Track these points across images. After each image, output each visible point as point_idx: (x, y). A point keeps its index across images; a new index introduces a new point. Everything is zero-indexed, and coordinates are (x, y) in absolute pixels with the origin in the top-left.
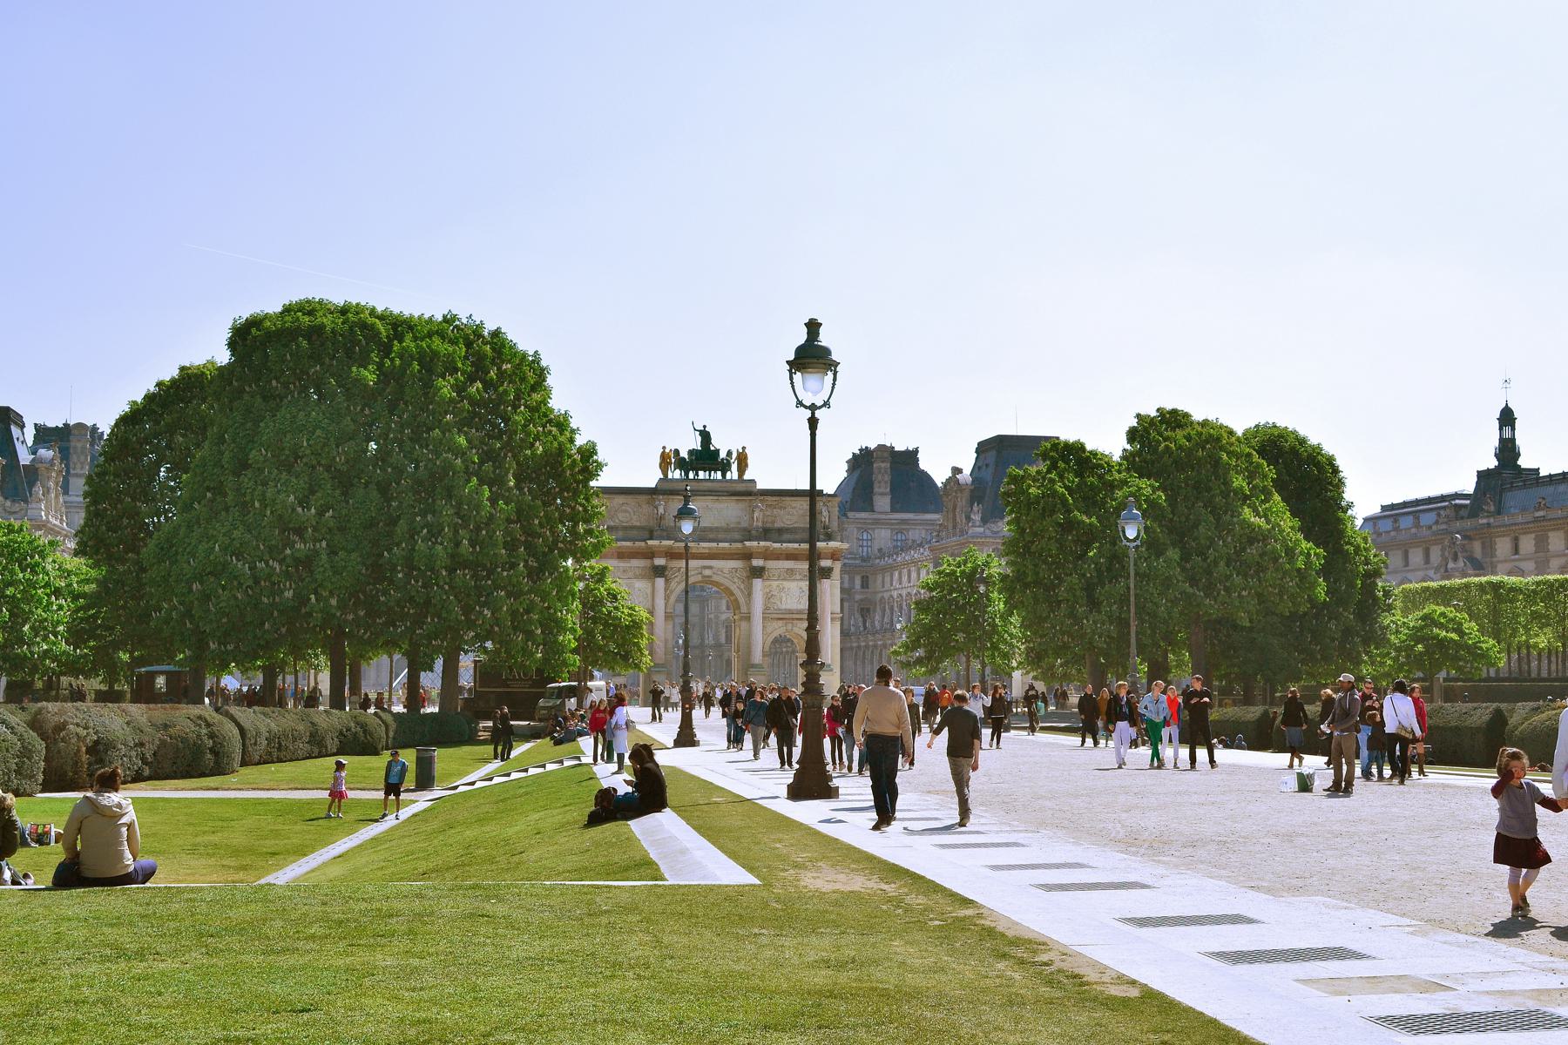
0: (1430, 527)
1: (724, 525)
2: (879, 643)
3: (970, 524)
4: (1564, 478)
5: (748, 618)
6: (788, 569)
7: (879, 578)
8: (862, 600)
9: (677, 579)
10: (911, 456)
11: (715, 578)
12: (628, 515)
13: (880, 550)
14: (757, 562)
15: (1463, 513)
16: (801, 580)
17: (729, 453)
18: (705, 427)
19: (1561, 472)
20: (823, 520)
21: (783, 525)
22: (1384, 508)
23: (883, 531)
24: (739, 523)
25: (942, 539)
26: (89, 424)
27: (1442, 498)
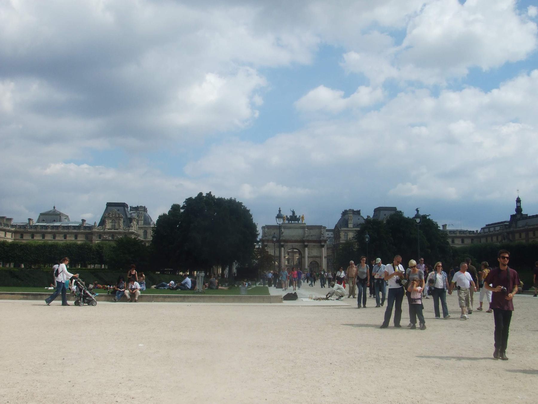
0: (498, 231)
4: (537, 216)
5: (304, 257)
11: (296, 248)
13: (350, 238)
14: (306, 244)
15: (507, 227)
16: (317, 248)
17: (300, 216)
18: (293, 210)
19: (532, 215)
22: (487, 225)
26: (143, 206)
27: (502, 222)
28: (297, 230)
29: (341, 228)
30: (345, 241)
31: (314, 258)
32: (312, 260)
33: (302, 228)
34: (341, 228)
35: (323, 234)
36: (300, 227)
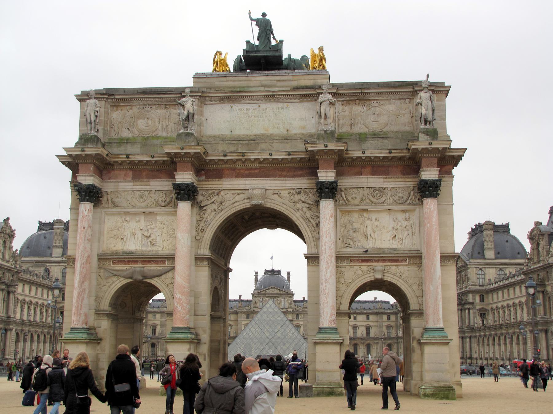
1: (285, 132)
2: (493, 333)
3: (550, 255)
6: (376, 189)
7: (490, 295)
8: (481, 309)
9: (214, 206)
10: (505, 228)
12: (150, 121)
13: (490, 280)
16: (396, 203)
18: (264, 15)
20: (424, 111)
21: (366, 130)
23: (491, 270)
24: (303, 128)
25: (530, 267)
28: (280, 105)
29: (469, 260)
30: (480, 286)
31: (379, 266)
32: (369, 278)
33: (303, 98)
34: (469, 260)
35: (426, 122)
36: (296, 88)
